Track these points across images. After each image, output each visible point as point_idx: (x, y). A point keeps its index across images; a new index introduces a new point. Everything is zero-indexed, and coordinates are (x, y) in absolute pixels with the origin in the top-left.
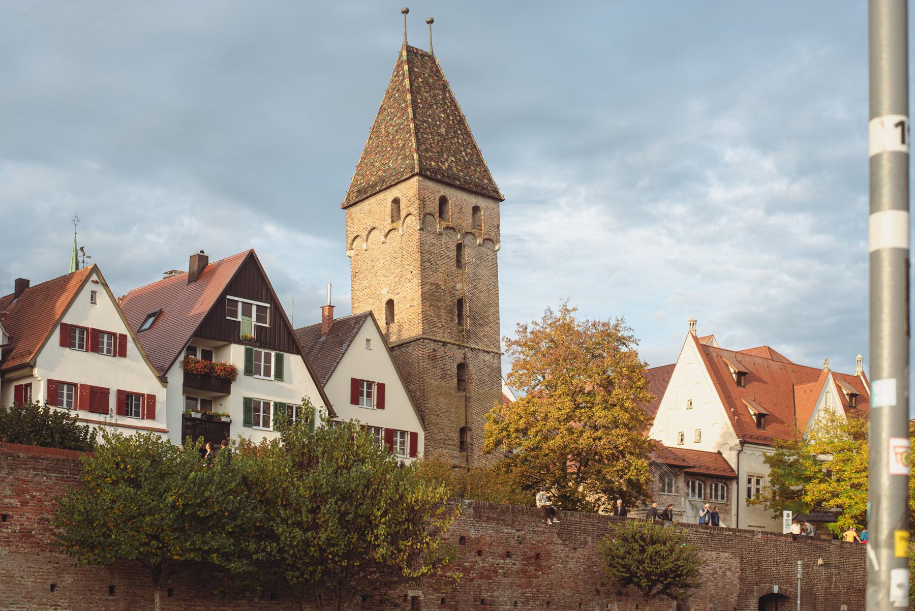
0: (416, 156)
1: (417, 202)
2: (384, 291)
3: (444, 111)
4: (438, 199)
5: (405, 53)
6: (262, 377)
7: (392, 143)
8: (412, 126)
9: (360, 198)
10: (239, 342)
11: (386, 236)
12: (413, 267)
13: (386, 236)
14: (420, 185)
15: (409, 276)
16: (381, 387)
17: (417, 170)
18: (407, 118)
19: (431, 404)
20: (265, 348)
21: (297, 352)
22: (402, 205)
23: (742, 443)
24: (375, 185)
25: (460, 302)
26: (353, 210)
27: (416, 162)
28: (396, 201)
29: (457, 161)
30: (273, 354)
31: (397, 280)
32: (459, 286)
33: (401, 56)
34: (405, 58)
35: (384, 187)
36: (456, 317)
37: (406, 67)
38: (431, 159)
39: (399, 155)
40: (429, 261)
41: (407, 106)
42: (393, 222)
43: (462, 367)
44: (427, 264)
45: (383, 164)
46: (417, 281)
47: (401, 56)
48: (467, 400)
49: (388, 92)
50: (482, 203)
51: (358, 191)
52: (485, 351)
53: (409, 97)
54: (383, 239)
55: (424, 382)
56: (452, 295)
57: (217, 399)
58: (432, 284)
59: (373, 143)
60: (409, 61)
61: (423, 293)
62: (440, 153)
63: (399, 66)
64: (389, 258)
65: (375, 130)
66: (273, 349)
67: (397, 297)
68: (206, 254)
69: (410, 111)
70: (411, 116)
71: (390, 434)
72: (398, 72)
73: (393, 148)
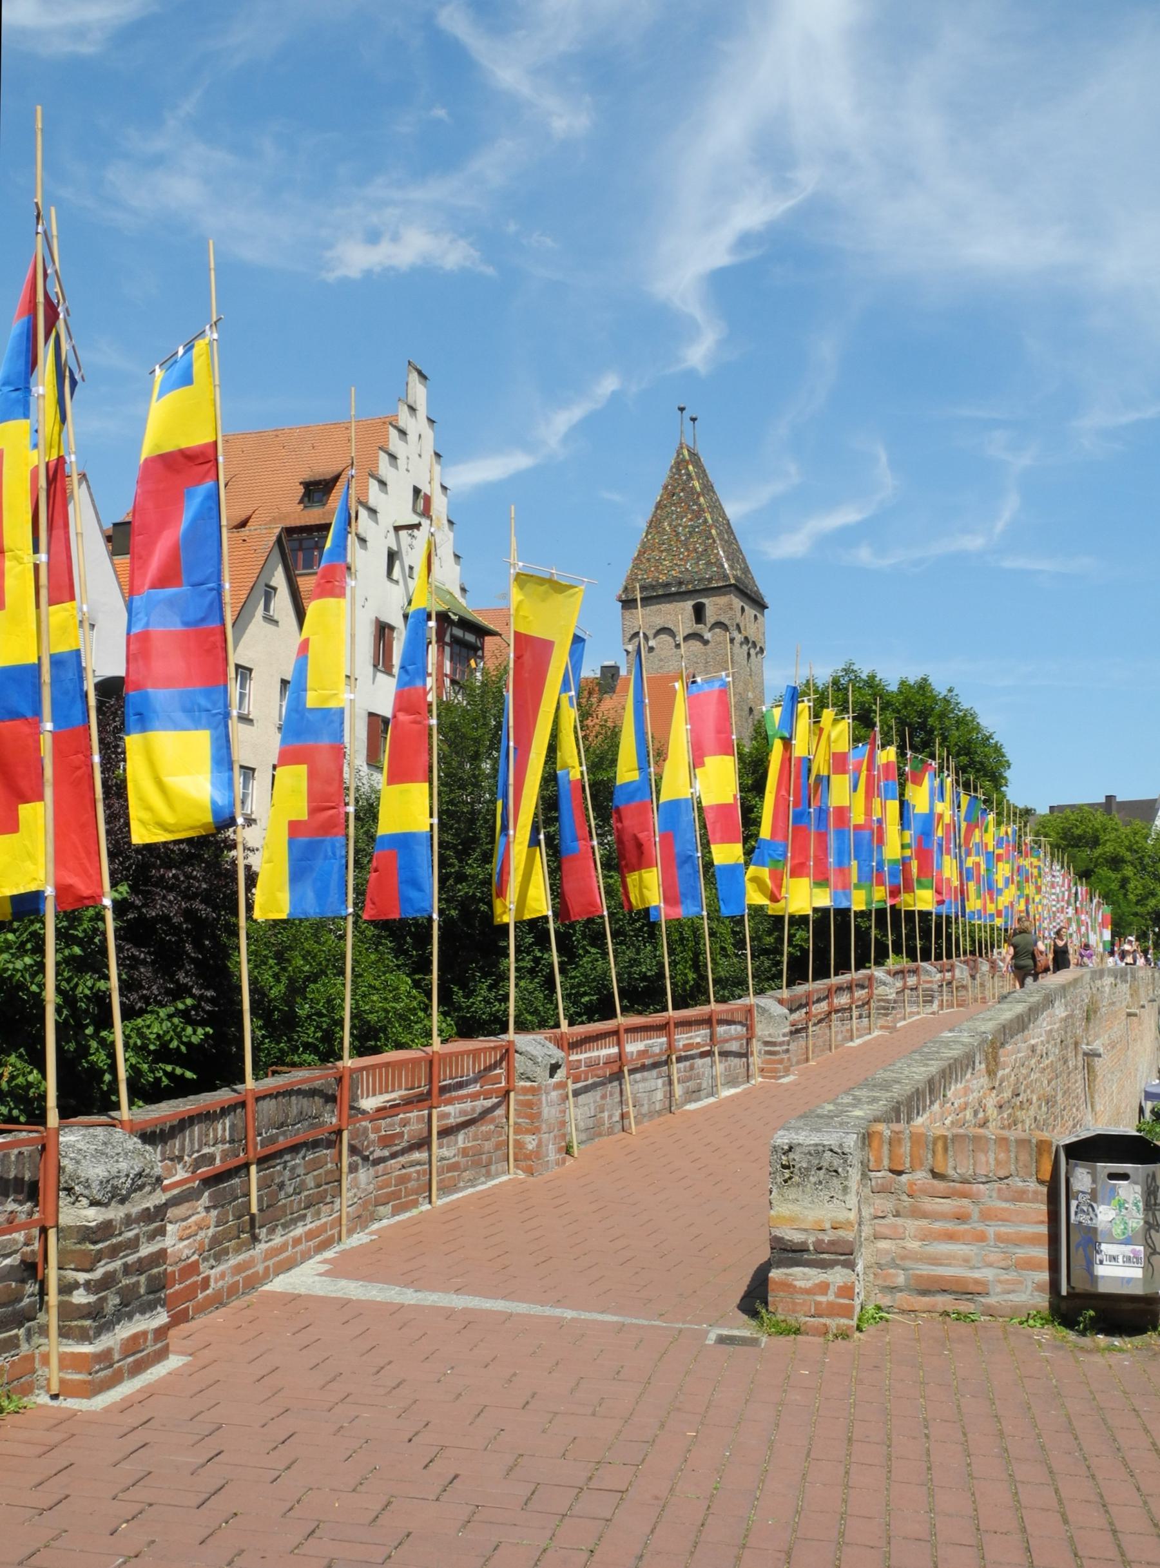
5: (686, 452)
7: (685, 545)
17: (733, 582)
18: (705, 521)
24: (667, 585)
33: (679, 453)
34: (687, 457)
35: (683, 588)
39: (699, 559)
49: (665, 488)
63: (680, 464)
70: (710, 521)
73: (688, 550)
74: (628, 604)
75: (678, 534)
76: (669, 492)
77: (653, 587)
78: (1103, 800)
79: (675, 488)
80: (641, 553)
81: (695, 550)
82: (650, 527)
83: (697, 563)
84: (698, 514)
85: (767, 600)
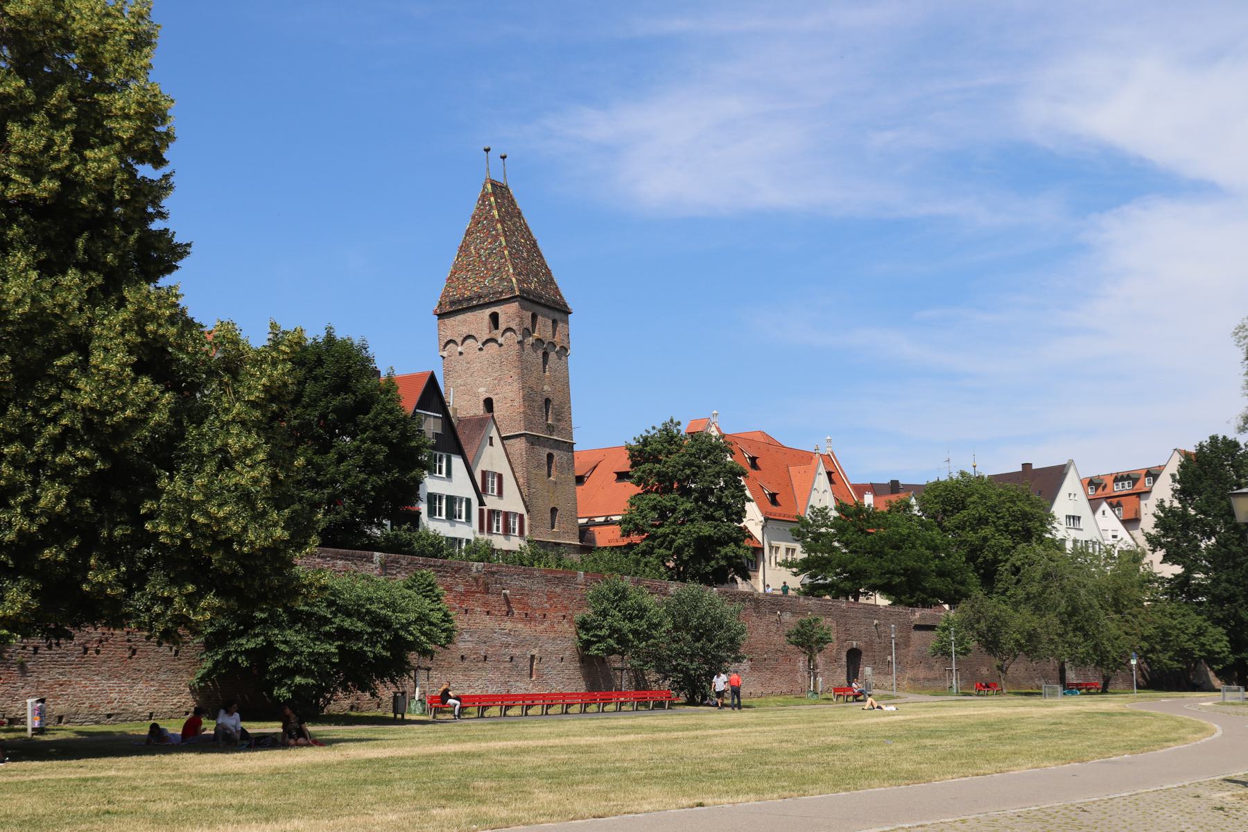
3: (523, 237)
5: (489, 186)
11: (484, 344)
13: (484, 344)
15: (510, 380)
16: (500, 477)
21: (461, 452)
22: (501, 320)
23: (766, 519)
24: (471, 299)
25: (548, 401)
28: (494, 318)
29: (539, 282)
32: (546, 388)
33: (484, 187)
37: (492, 199)
38: (524, 281)
41: (498, 234)
46: (516, 386)
47: (484, 187)
49: (473, 217)
50: (557, 316)
51: (452, 303)
53: (499, 226)
60: (494, 194)
62: (528, 275)
63: (484, 196)
65: (464, 249)
69: (502, 239)
71: (507, 515)
74: (441, 316)
76: (476, 221)
77: (460, 302)
78: (1020, 469)
80: (453, 273)
81: (492, 268)
84: (496, 238)
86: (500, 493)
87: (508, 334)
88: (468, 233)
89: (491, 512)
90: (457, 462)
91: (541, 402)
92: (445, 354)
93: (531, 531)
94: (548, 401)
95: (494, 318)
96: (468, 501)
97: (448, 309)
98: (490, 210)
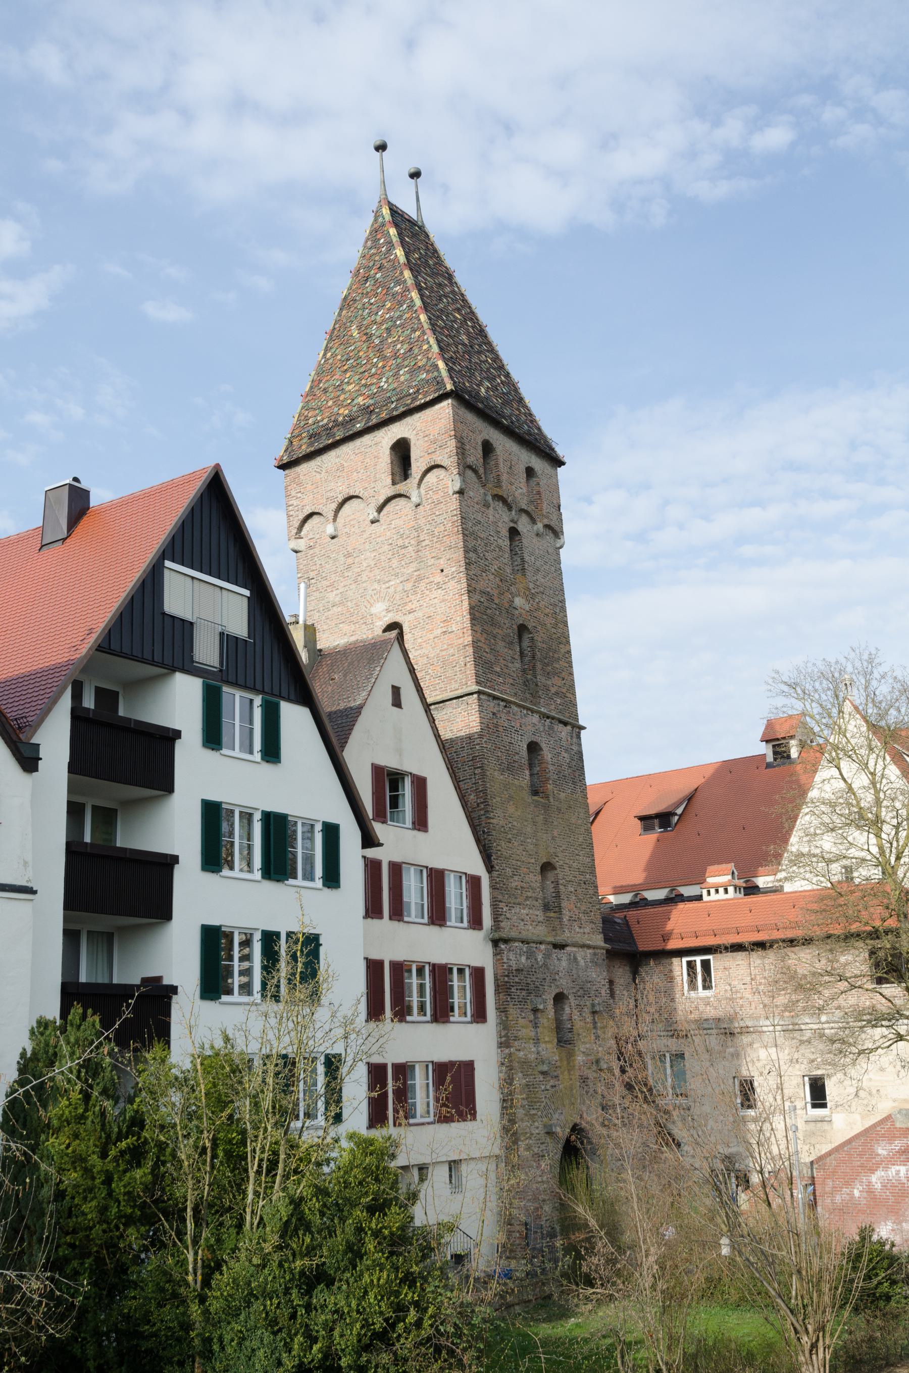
0: (441, 364)
1: (452, 443)
2: (379, 608)
4: (480, 443)
5: (386, 211)
6: (237, 753)
7: (380, 351)
8: (423, 317)
9: (317, 446)
10: (190, 668)
11: (380, 509)
12: (452, 560)
13: (380, 509)
14: (455, 414)
15: (438, 578)
16: (420, 784)
17: (449, 387)
18: (411, 306)
19: (498, 819)
20: (245, 687)
22: (415, 454)
24: (352, 419)
26: (303, 469)
27: (444, 373)
30: (258, 700)
31: (408, 586)
32: (518, 601)
33: (377, 214)
35: (374, 420)
36: (517, 657)
39: (399, 367)
40: (475, 551)
42: (394, 483)
43: (533, 748)
44: (472, 555)
45: (365, 385)
48: (547, 807)
50: (538, 464)
51: (313, 436)
52: (561, 722)
53: (407, 274)
54: (373, 514)
55: (483, 775)
56: (512, 617)
57: (133, 804)
58: (483, 592)
59: (334, 356)
61: (472, 608)
63: (376, 231)
64: (386, 548)
66: (262, 692)
67: (411, 617)
68: (84, 485)
69: (415, 295)
70: (418, 303)
72: (376, 241)
73: (384, 358)
75: (369, 336)
77: (328, 430)
79: (370, 268)
80: (315, 384)
81: (395, 356)
82: (331, 339)
83: (396, 375)
85: (560, 451)
86: (421, 823)
87: (431, 477)
88: (347, 303)
89: (396, 869)
90: (295, 720)
91: (508, 628)
92: (301, 544)
93: (497, 916)
94: (522, 629)
95: (402, 451)
96: (331, 832)
97: (305, 449)
98: (389, 251)
